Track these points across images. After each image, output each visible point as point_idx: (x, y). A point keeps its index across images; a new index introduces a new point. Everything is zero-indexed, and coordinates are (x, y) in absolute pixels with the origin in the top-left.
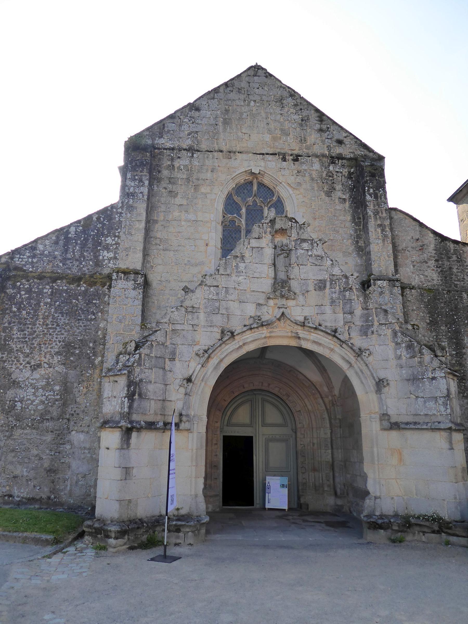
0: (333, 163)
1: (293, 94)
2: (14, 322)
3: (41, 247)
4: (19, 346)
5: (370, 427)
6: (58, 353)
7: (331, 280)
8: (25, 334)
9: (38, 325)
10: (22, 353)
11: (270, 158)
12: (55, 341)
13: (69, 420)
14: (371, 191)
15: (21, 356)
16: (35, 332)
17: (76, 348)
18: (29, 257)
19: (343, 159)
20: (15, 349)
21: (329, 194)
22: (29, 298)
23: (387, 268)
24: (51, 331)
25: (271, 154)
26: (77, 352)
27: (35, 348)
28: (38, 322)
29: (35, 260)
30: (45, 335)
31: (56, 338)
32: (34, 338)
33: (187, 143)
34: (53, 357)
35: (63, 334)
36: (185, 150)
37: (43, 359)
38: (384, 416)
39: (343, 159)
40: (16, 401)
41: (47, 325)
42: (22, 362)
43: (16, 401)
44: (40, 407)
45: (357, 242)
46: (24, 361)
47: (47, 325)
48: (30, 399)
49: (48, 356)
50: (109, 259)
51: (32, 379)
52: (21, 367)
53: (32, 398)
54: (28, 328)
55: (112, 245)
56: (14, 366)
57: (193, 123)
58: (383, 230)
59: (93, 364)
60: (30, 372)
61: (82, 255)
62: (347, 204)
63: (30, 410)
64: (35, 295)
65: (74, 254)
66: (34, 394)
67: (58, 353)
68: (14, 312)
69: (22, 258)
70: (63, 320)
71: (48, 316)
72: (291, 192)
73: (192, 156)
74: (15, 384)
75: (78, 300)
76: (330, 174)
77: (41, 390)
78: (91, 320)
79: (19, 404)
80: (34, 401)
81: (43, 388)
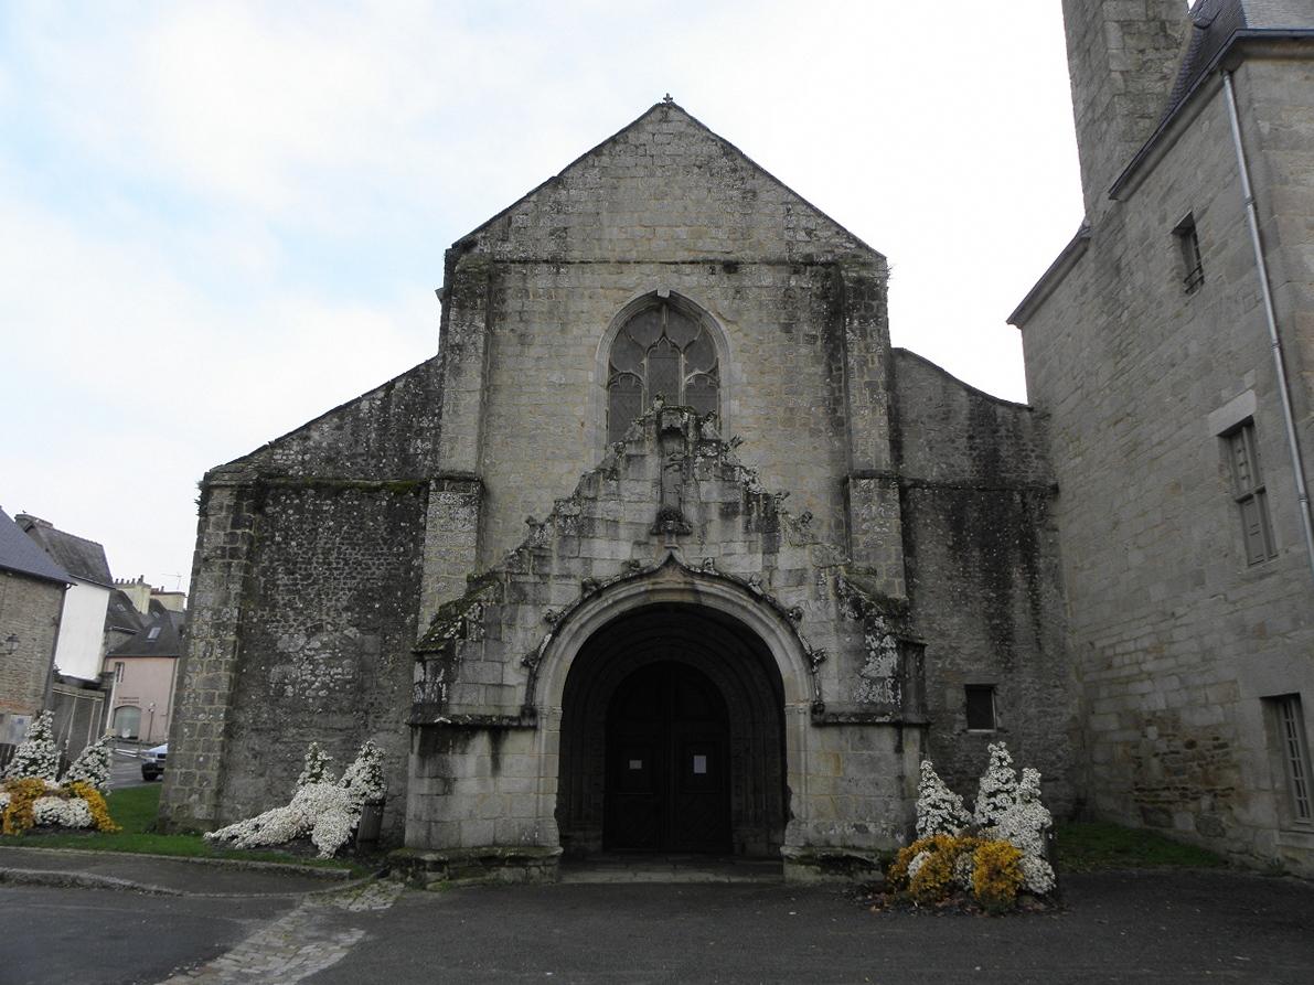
0: (796, 272)
1: (729, 150)
2: (278, 560)
3: (315, 435)
5: (798, 720)
6: (346, 609)
7: (748, 502)
8: (296, 579)
10: (293, 609)
11: (687, 269)
12: (343, 589)
13: (366, 713)
14: (856, 323)
15: (291, 613)
16: (312, 575)
17: (375, 600)
18: (297, 453)
20: (282, 602)
21: (787, 328)
22: (300, 521)
23: (878, 460)
24: (336, 573)
25: (692, 263)
26: (377, 606)
27: (312, 600)
29: (307, 457)
30: (326, 579)
33: (548, 248)
34: (340, 615)
35: (354, 578)
36: (547, 262)
37: (324, 617)
38: (817, 709)
39: (812, 264)
42: (292, 622)
43: (286, 684)
44: (321, 693)
45: (835, 411)
48: (305, 681)
49: (332, 613)
50: (425, 454)
51: (310, 650)
52: (292, 630)
54: (300, 569)
55: (429, 429)
56: (281, 631)
57: (558, 212)
58: (873, 392)
59: (403, 624)
63: (307, 698)
65: (368, 446)
66: (313, 673)
67: (346, 609)
68: (279, 543)
70: (355, 555)
71: (330, 548)
72: (723, 327)
73: (558, 272)
74: (285, 658)
75: (375, 520)
76: (788, 295)
77: (323, 667)
79: (290, 689)
80: (313, 683)
81: (327, 663)
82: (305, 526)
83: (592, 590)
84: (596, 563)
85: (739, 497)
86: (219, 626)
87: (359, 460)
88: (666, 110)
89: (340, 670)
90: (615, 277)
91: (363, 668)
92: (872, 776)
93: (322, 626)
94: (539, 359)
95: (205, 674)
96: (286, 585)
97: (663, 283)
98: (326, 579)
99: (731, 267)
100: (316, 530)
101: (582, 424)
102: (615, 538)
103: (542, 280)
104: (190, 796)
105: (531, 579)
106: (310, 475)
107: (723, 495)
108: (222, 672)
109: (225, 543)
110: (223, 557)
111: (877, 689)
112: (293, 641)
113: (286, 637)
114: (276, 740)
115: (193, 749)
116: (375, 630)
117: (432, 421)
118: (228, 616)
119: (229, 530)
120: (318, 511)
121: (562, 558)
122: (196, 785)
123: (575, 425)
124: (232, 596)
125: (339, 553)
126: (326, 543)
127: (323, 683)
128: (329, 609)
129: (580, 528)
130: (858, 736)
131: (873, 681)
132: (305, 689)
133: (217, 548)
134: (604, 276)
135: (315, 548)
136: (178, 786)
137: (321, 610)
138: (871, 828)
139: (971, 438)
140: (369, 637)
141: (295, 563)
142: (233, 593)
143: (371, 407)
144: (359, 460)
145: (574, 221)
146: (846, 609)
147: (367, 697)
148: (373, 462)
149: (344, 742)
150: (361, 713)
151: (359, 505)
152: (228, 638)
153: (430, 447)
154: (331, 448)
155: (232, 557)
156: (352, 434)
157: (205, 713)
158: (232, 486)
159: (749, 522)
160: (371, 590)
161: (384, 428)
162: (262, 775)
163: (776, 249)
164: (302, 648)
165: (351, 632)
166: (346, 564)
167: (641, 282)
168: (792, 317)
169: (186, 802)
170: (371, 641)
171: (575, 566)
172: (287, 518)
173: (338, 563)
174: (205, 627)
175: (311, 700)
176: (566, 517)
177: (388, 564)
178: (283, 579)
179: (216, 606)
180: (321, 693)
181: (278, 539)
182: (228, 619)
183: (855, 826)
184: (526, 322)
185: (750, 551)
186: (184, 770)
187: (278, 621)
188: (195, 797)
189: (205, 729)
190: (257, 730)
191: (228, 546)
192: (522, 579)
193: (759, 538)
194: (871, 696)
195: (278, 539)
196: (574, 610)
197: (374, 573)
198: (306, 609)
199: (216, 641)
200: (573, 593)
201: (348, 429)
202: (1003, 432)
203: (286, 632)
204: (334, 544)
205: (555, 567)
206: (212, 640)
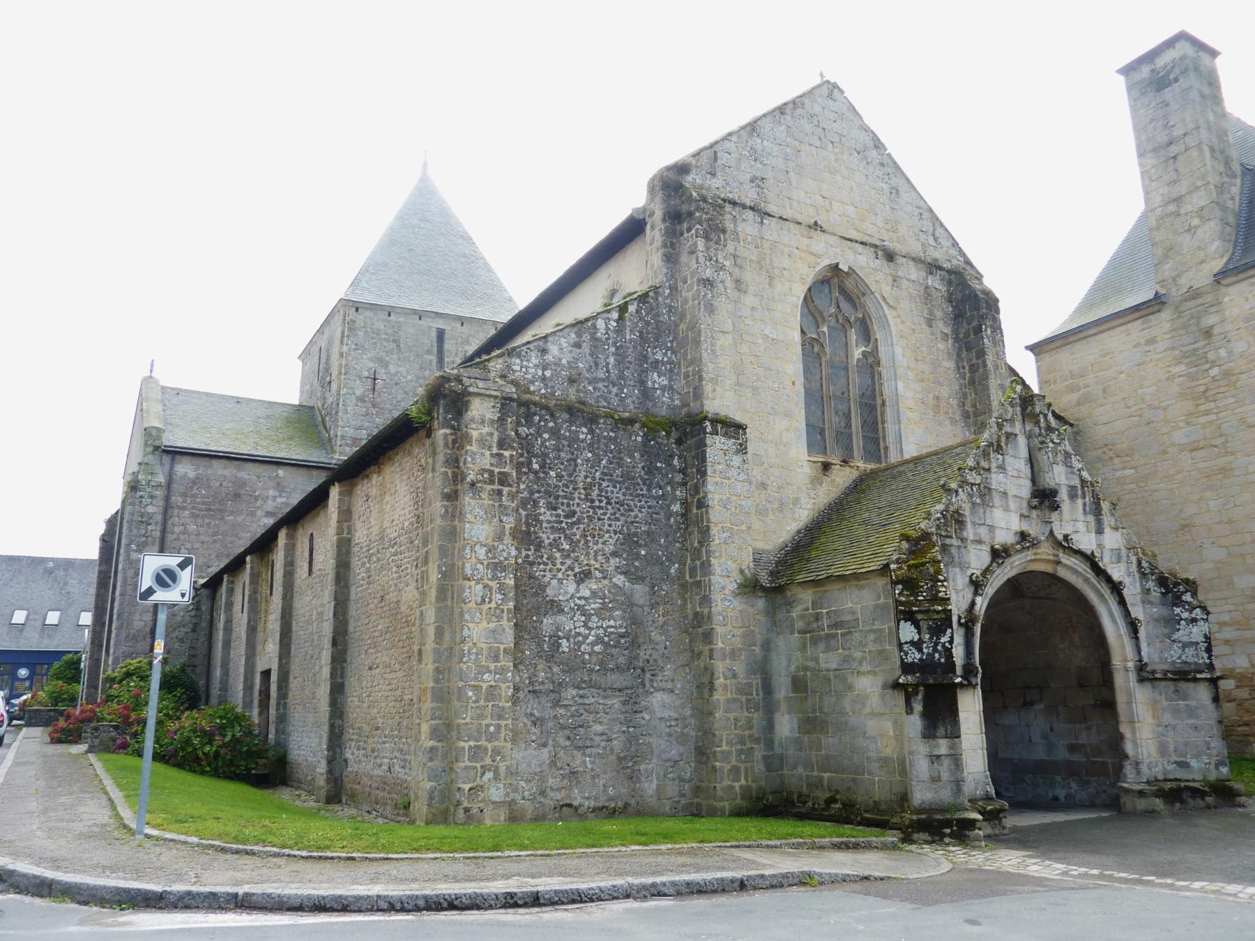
0: (931, 273)
2: (539, 492)
4: (552, 537)
5: (1124, 680)
6: (615, 554)
7: (1083, 488)
9: (577, 501)
10: (559, 550)
11: (860, 248)
12: (608, 531)
15: (558, 555)
16: (575, 512)
17: (640, 546)
18: (536, 366)
19: (940, 268)
20: (547, 542)
21: (930, 323)
22: (558, 449)
24: (600, 512)
25: (862, 243)
26: (643, 553)
27: (579, 541)
28: (576, 495)
29: (548, 373)
31: (610, 525)
32: (574, 523)
35: (618, 519)
36: (752, 208)
37: (592, 562)
38: (1141, 667)
40: (560, 638)
41: (592, 501)
42: (559, 566)
43: (560, 638)
44: (597, 648)
45: (964, 404)
46: (562, 564)
47: (592, 501)
48: (579, 634)
49: (599, 558)
50: (663, 389)
51: (580, 598)
52: (560, 575)
53: (582, 630)
55: (663, 363)
59: (668, 575)
60: (575, 586)
61: (621, 377)
62: (950, 341)
63: (583, 653)
64: (566, 443)
65: (608, 371)
66: (586, 625)
67: (615, 554)
68: (536, 472)
69: (526, 367)
70: (617, 495)
72: (887, 312)
73: (762, 222)
74: (555, 607)
75: (632, 457)
77: (595, 619)
78: (658, 498)
79: (564, 642)
80: (586, 637)
82: (562, 454)
83: (999, 554)
84: (998, 532)
85: (1077, 482)
86: (497, 567)
87: (600, 385)
88: (831, 89)
89: (612, 623)
90: (806, 241)
91: (635, 621)
92: (1192, 721)
93: (590, 572)
94: (753, 309)
95: (484, 624)
96: (549, 522)
97: (851, 258)
99: (890, 256)
100: (575, 460)
101: (794, 383)
102: (1007, 510)
103: (748, 226)
104: (483, 774)
105: (955, 542)
106: (553, 394)
107: (1067, 478)
108: (505, 622)
109: (491, 465)
110: (492, 482)
111: (1190, 651)
112: (564, 589)
113: (554, 582)
114: (556, 704)
115: (481, 717)
116: (643, 579)
117: (665, 354)
118: (505, 554)
119: (495, 450)
120: (574, 439)
121: (974, 524)
122: (488, 761)
123: (788, 383)
124: (507, 532)
125: (601, 490)
126: (586, 477)
127: (597, 636)
128: (596, 553)
129: (982, 496)
130: (1172, 688)
131: (1185, 645)
132: (579, 644)
133: (484, 470)
134: (790, 237)
135: (576, 483)
136: (468, 763)
137: (587, 554)
138: (1193, 763)
140: (636, 586)
141: (557, 497)
142: (508, 526)
143: (607, 329)
144: (600, 385)
145: (769, 174)
146: (1151, 584)
147: (642, 653)
148: (615, 390)
149: (624, 703)
150: (639, 671)
151: (616, 437)
152: (507, 581)
153: (666, 382)
154: (571, 367)
155: (502, 483)
156: (591, 355)
157: (490, 672)
158: (496, 397)
159: (1085, 504)
160: (636, 534)
161: (620, 355)
162: (545, 745)
163: (915, 248)
164: (572, 597)
165: (619, 580)
166: (609, 503)
167: (829, 252)
168: (931, 313)
169: (478, 782)
170: (640, 592)
171: (983, 532)
172: (543, 443)
173: (601, 501)
174: (479, 566)
175: (587, 657)
176: (973, 484)
177: (650, 507)
178: (546, 515)
179: (490, 542)
180: (597, 648)
182: (506, 559)
183: (1176, 762)
184: (741, 267)
185: (1088, 531)
186: (472, 743)
187: (546, 564)
188: (489, 775)
189: (492, 693)
190: (534, 692)
191: (497, 470)
192: (948, 541)
193: (1091, 518)
194: (1183, 658)
195: (536, 466)
196: (987, 571)
197: (636, 517)
198: (574, 551)
199: (494, 584)
200: (986, 558)
201: (586, 348)
203: (554, 577)
204: (594, 478)
205: (969, 533)
206: (490, 583)
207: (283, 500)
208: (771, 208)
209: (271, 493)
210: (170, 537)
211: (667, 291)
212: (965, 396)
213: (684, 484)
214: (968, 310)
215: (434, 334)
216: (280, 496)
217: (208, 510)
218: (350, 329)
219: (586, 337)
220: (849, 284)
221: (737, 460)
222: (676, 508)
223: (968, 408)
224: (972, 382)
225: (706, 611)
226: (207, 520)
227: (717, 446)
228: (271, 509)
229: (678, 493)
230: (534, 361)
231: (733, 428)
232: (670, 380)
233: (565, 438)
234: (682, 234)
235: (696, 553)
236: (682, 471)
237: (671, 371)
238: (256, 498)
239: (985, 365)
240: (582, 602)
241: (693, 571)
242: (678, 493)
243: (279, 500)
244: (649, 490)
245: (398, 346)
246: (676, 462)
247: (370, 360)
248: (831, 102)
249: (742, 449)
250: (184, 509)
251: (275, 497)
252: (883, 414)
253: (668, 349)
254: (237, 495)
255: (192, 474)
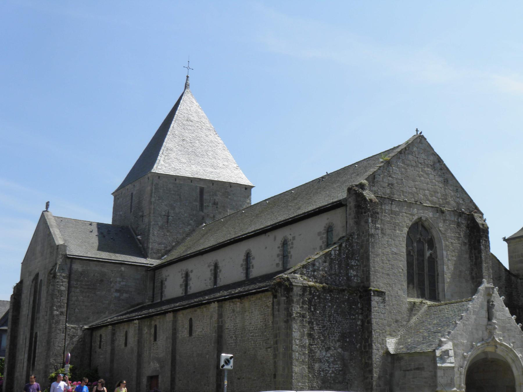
1: (440, 160)
3: (317, 264)
6: (338, 341)
13: (347, 383)
18: (311, 271)
22: (320, 303)
24: (334, 325)
41: (331, 321)
44: (333, 375)
45: (472, 273)
47: (331, 321)
48: (326, 370)
50: (355, 276)
53: (328, 369)
55: (355, 266)
59: (356, 348)
61: (340, 273)
62: (467, 246)
67: (338, 341)
68: (313, 312)
70: (339, 319)
72: (441, 236)
75: (344, 304)
78: (353, 319)
79: (322, 373)
80: (329, 371)
81: (333, 362)
87: (333, 276)
89: (337, 366)
98: (330, 328)
119: (301, 305)
120: (326, 299)
125: (334, 317)
132: (327, 373)
139: (506, 287)
140: (345, 353)
143: (335, 254)
145: (395, 182)
153: (355, 274)
161: (340, 265)
164: (325, 356)
165: (340, 350)
166: (336, 322)
167: (417, 213)
170: (347, 354)
180: (333, 375)
181: (312, 309)
202: (513, 286)
204: (331, 313)
207: (124, 283)
208: (396, 197)
209: (118, 279)
210: (71, 303)
211: (356, 236)
212: (472, 270)
213: (362, 314)
214: (475, 232)
215: (198, 190)
216: (123, 281)
217: (88, 288)
218: (155, 189)
219: (328, 258)
220: (426, 224)
221: (382, 306)
222: (359, 323)
223: (474, 274)
224: (476, 264)
225: (370, 362)
226: (87, 294)
227: (375, 300)
228: (118, 288)
229: (360, 317)
230: (311, 269)
231: (381, 294)
232: (357, 272)
233: (322, 298)
234: (362, 213)
235: (366, 340)
236: (362, 309)
237: (357, 269)
238: (111, 282)
239: (481, 257)
240: (327, 359)
241: (365, 347)
242: (360, 317)
243: (122, 283)
244: (350, 317)
245: (180, 197)
246: (359, 305)
247: (166, 205)
248: (420, 145)
249: (384, 301)
250: (76, 288)
251: (120, 282)
252: (438, 278)
253: (356, 260)
254: (102, 281)
255: (80, 270)
